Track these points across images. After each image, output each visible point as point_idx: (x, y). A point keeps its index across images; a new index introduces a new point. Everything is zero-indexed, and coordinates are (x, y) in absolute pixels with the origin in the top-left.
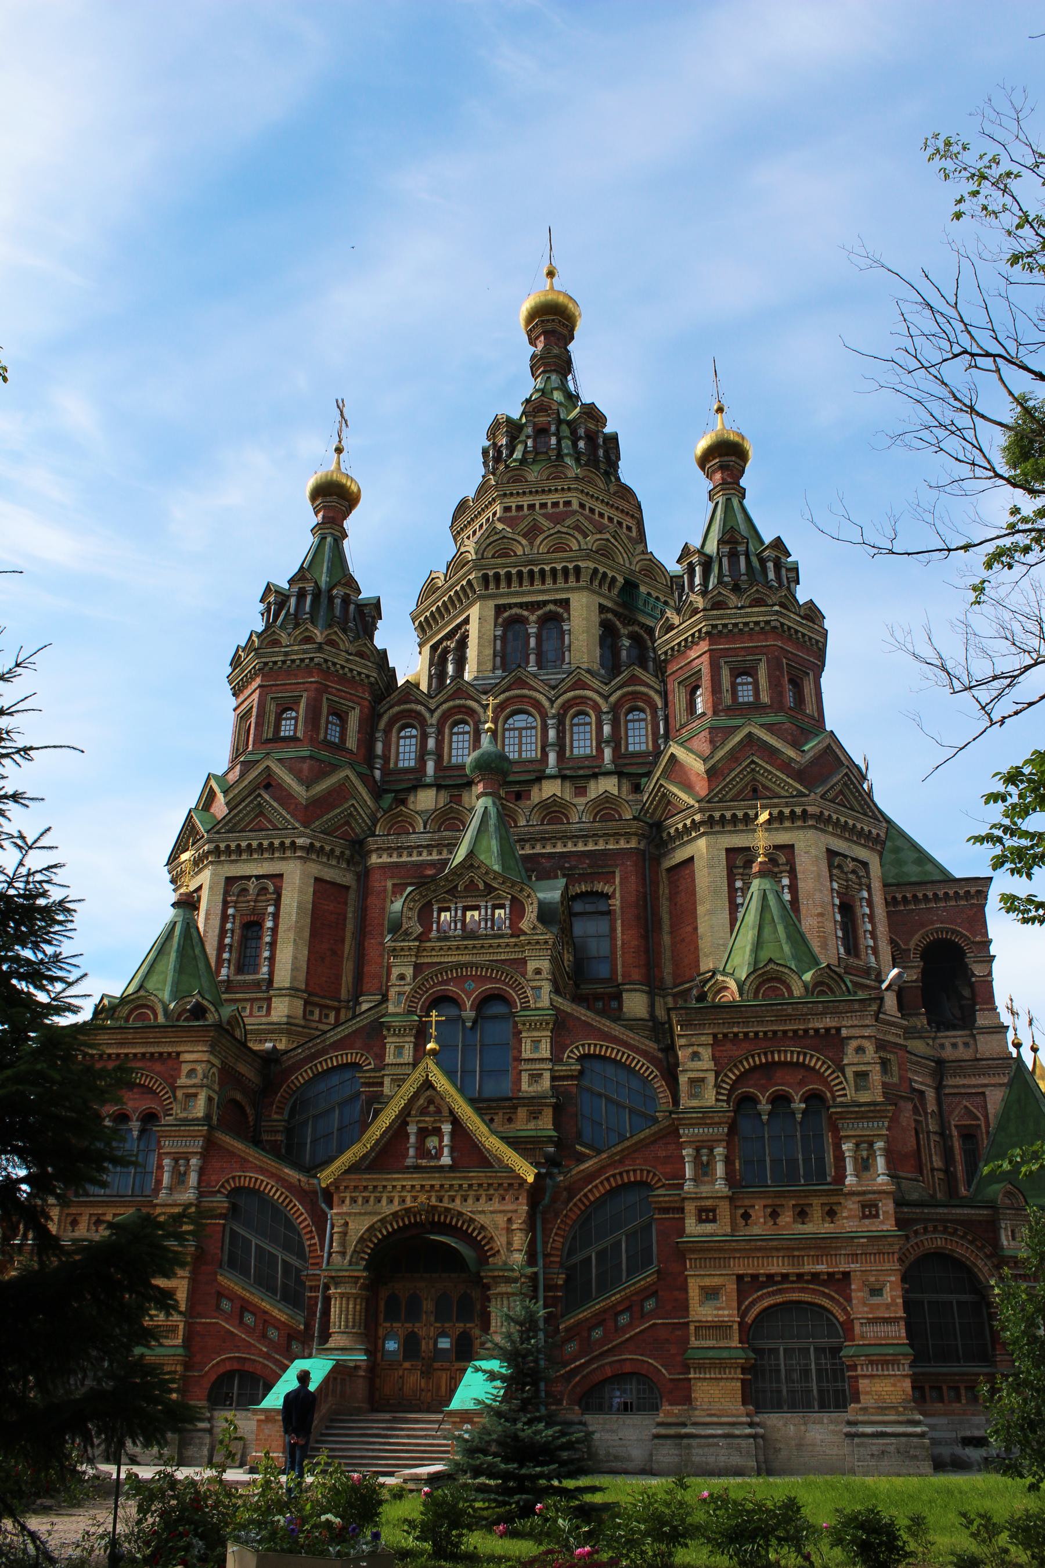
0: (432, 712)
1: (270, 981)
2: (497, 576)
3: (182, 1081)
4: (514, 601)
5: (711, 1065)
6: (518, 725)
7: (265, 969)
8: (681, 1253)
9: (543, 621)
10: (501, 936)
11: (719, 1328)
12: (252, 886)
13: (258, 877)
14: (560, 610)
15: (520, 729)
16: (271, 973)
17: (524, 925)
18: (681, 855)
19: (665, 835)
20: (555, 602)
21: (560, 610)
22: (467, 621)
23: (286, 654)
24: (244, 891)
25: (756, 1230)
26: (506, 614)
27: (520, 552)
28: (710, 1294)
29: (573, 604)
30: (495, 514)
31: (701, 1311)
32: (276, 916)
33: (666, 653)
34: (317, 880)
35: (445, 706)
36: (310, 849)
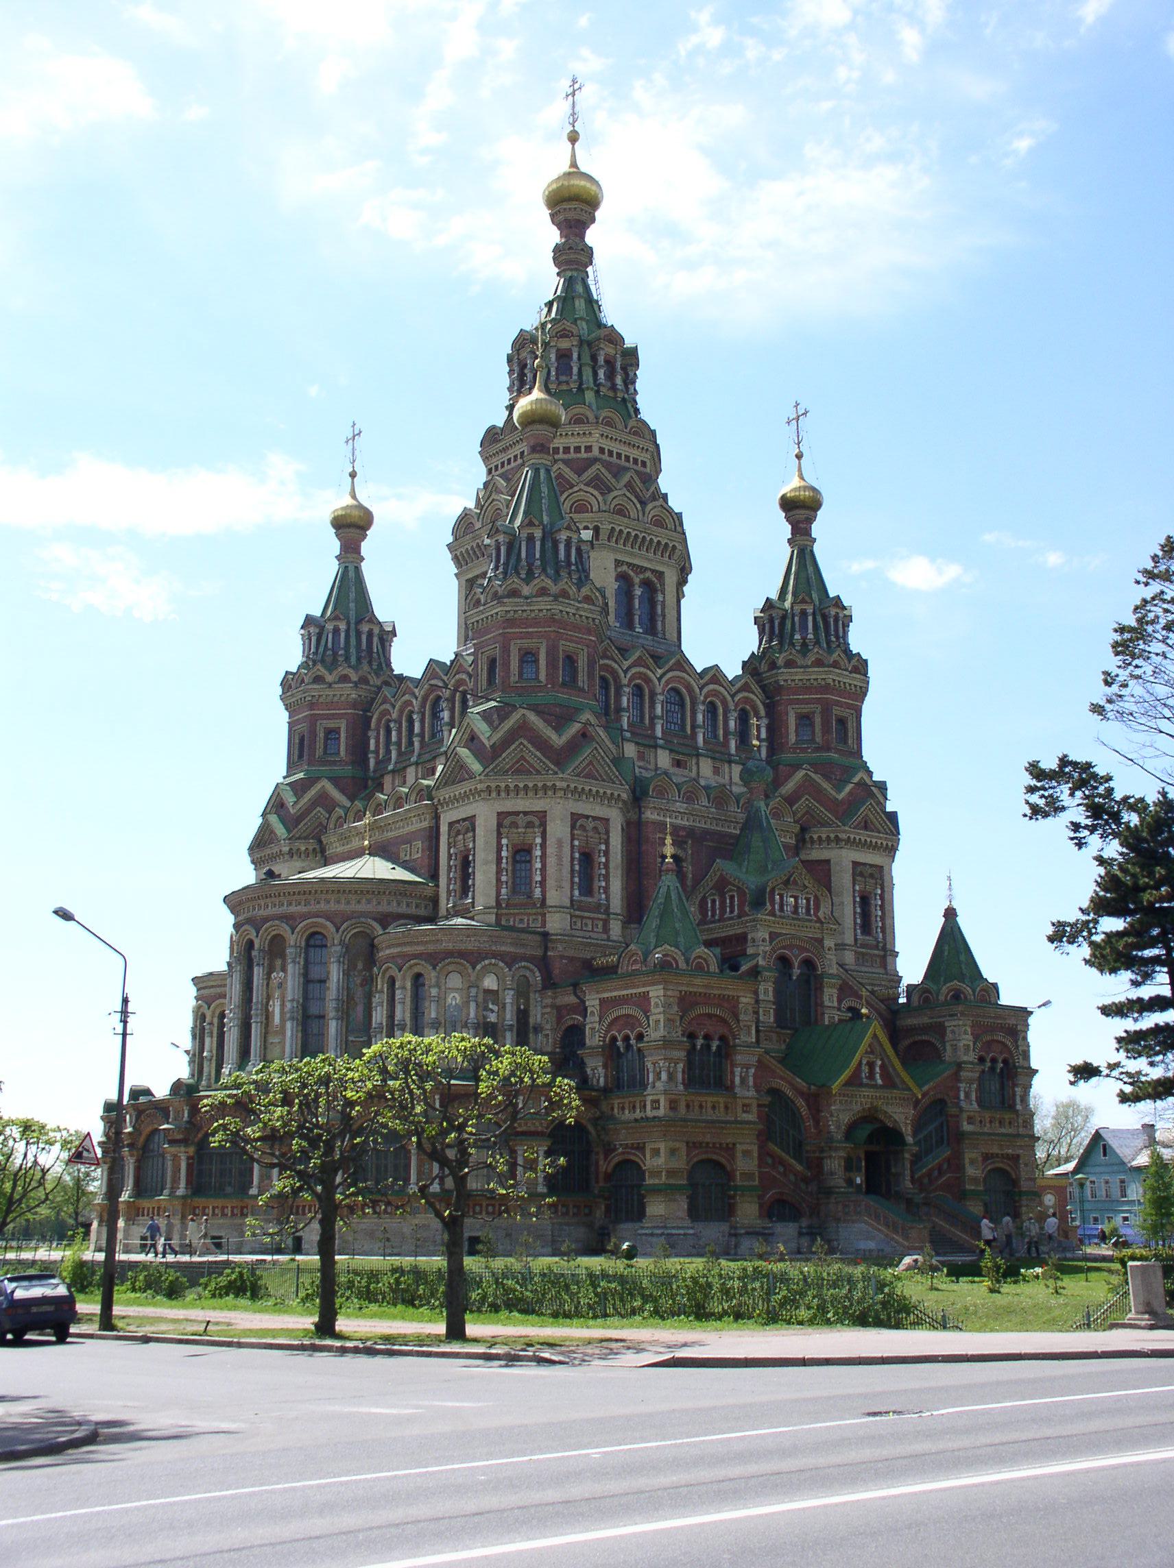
0: (625, 672)
1: (608, 907)
3: (742, 1017)
4: (627, 560)
5: (970, 1037)
8: (960, 1137)
10: (810, 921)
11: (975, 1180)
16: (608, 899)
17: (821, 914)
18: (816, 854)
19: (807, 837)
20: (653, 571)
23: (578, 609)
25: (986, 1130)
27: (633, 514)
28: (972, 1162)
30: (589, 449)
31: (971, 1171)
32: (606, 853)
33: (786, 681)
35: (634, 670)
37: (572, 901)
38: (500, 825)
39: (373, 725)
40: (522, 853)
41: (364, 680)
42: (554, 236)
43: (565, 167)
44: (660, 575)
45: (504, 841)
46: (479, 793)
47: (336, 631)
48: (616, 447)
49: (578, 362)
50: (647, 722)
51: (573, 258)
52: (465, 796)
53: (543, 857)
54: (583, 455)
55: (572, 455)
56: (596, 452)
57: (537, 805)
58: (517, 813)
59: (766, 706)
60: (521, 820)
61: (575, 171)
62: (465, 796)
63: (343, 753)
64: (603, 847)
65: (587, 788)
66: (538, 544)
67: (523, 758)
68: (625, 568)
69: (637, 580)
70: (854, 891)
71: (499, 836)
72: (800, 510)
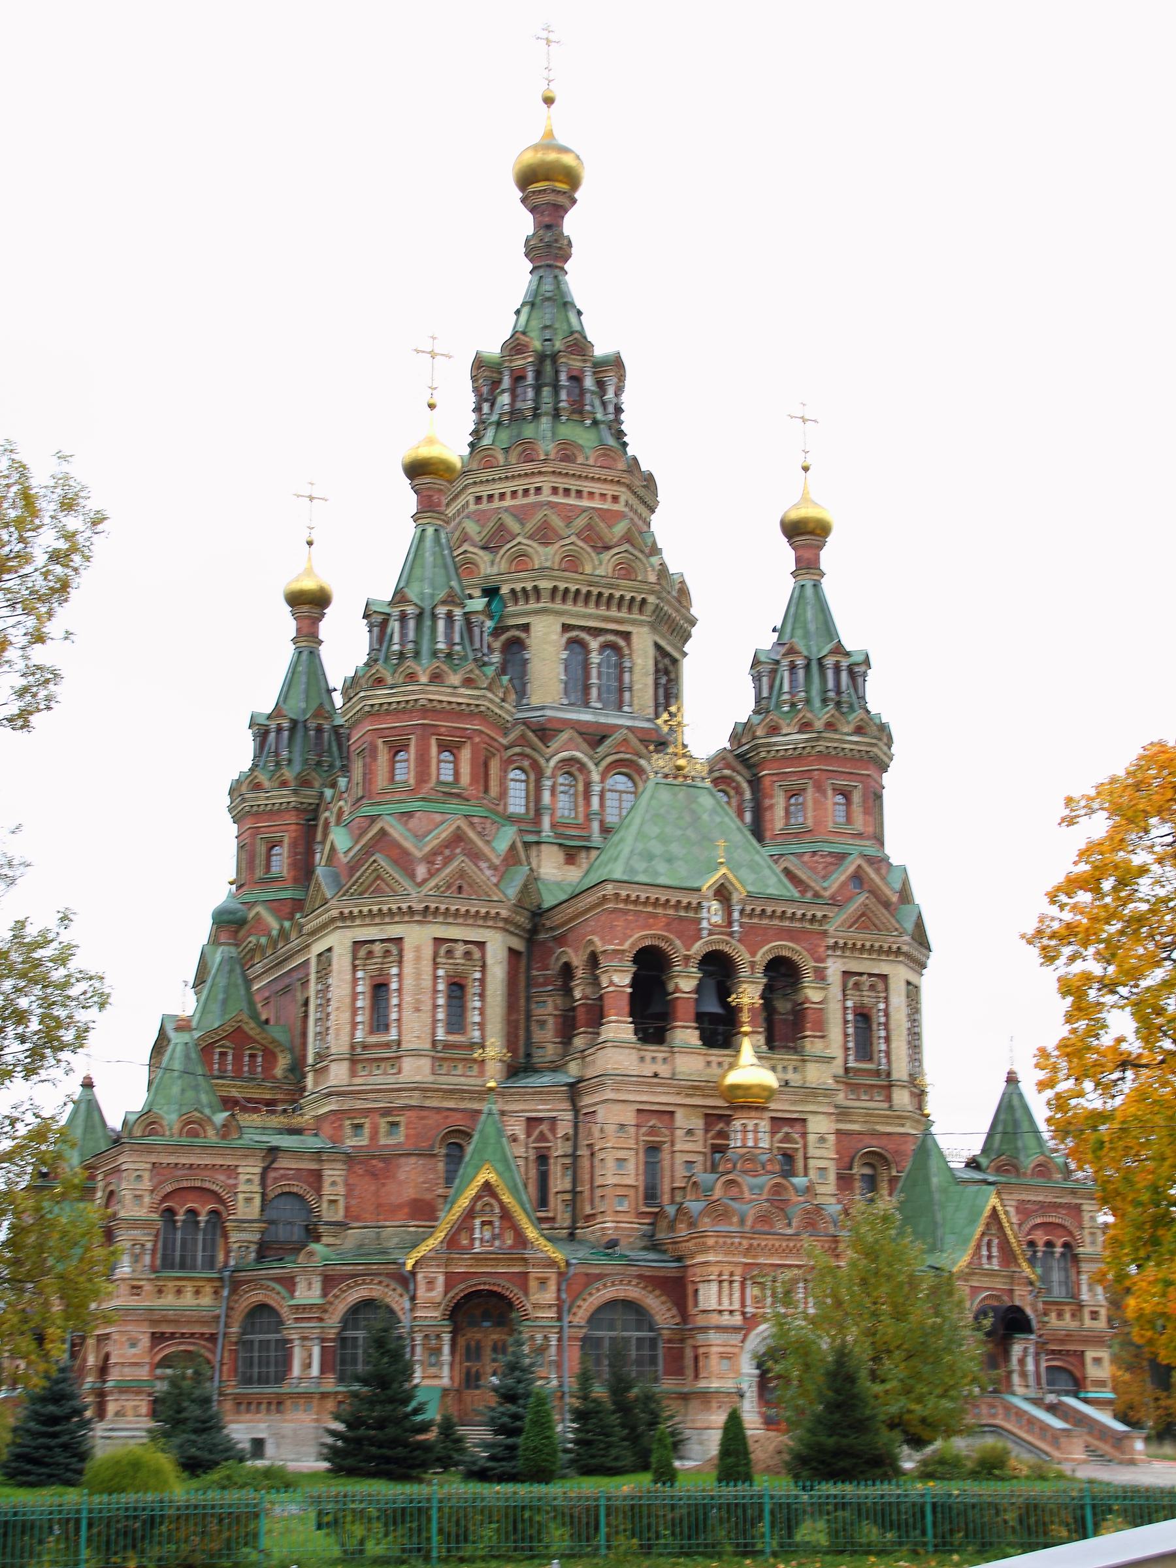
2: (567, 590)
6: (620, 787)
7: (477, 1034)
9: (605, 646)
12: (460, 949)
13: (466, 942)
14: (622, 643)
15: (621, 792)
21: (622, 643)
22: (526, 628)
24: (449, 953)
26: (568, 635)
27: (588, 569)
29: (635, 639)
32: (482, 981)
34: (511, 950)
36: (506, 920)
37: (434, 1043)
38: (355, 958)
39: (319, 838)
40: (379, 989)
41: (304, 783)
42: (525, 224)
43: (536, 139)
44: (627, 636)
45: (360, 974)
46: (333, 920)
47: (279, 729)
48: (574, 484)
49: (548, 382)
50: (581, 820)
51: (548, 251)
52: (324, 926)
53: (399, 990)
54: (532, 499)
55: (520, 501)
56: (546, 490)
57: (394, 931)
58: (372, 942)
59: (749, 782)
60: (377, 948)
61: (549, 143)
62: (324, 926)
63: (285, 873)
64: (478, 975)
65: (453, 908)
66: (411, 624)
67: (379, 877)
68: (574, 634)
69: (594, 644)
70: (845, 1008)
71: (355, 968)
72: (805, 535)
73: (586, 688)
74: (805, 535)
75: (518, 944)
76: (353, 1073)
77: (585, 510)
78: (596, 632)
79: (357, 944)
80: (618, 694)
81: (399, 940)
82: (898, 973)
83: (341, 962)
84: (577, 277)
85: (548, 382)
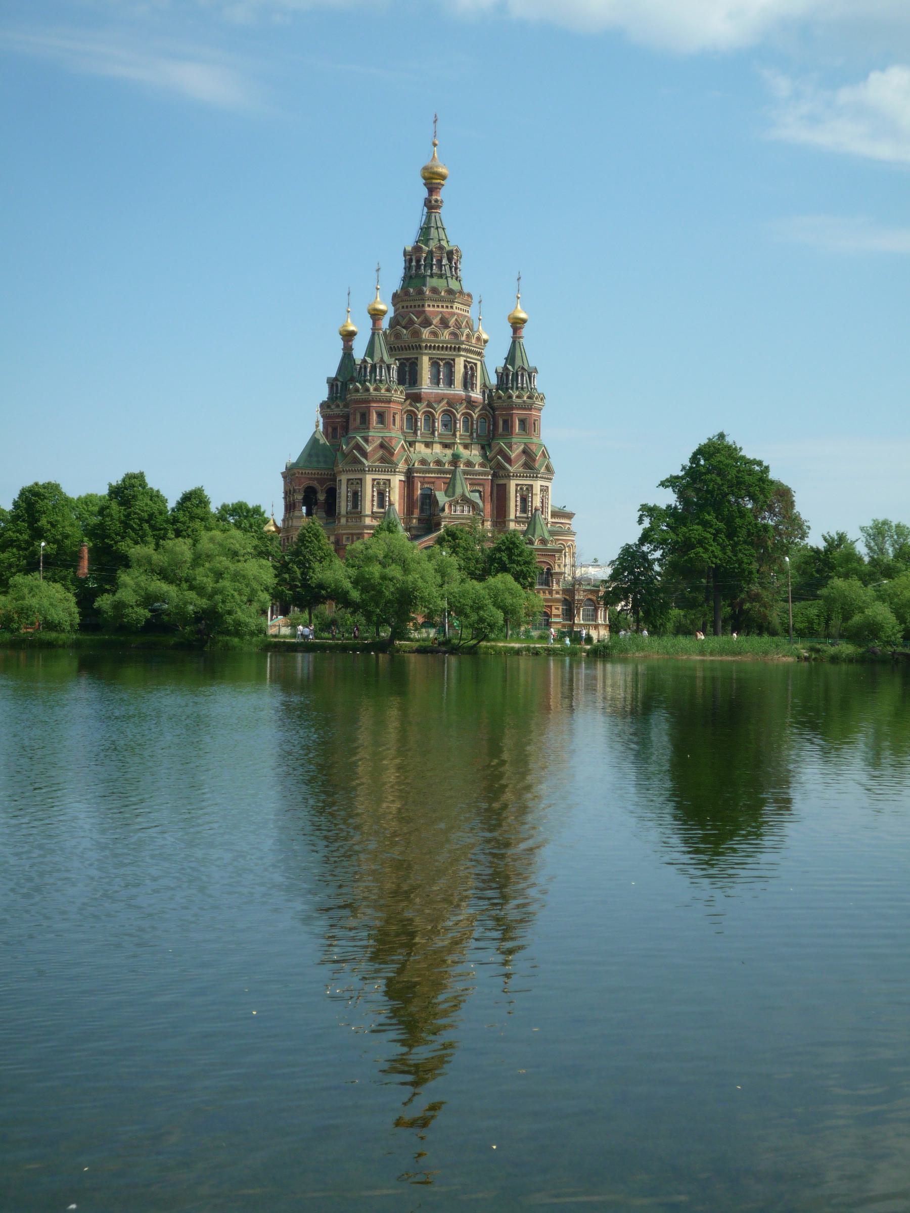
22: (417, 358)
37: (372, 512)
40: (355, 494)
69: (442, 364)
73: (439, 380)
74: (517, 325)
75: (403, 478)
76: (347, 521)
77: (441, 312)
78: (442, 360)
79: (348, 480)
80: (450, 382)
81: (361, 480)
82: (538, 485)
83: (344, 483)
84: (445, 214)
85: (427, 267)
